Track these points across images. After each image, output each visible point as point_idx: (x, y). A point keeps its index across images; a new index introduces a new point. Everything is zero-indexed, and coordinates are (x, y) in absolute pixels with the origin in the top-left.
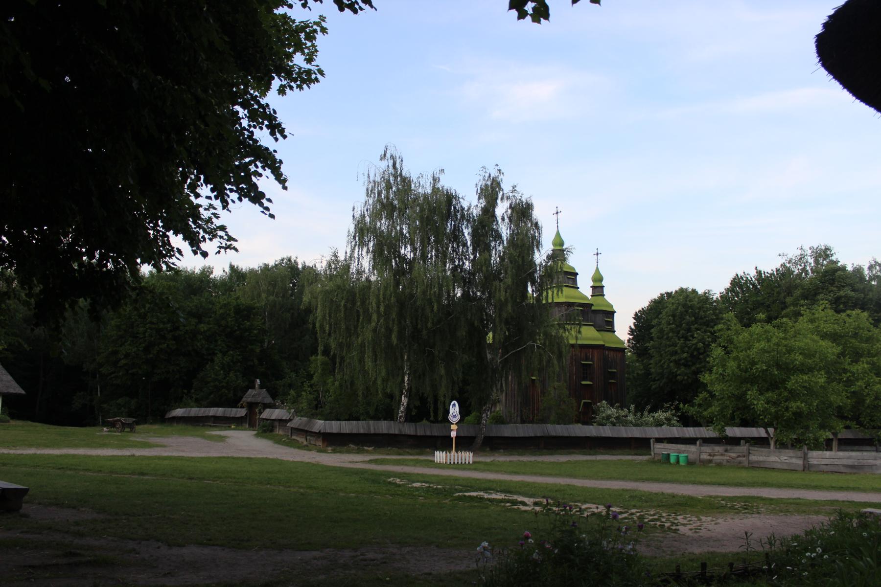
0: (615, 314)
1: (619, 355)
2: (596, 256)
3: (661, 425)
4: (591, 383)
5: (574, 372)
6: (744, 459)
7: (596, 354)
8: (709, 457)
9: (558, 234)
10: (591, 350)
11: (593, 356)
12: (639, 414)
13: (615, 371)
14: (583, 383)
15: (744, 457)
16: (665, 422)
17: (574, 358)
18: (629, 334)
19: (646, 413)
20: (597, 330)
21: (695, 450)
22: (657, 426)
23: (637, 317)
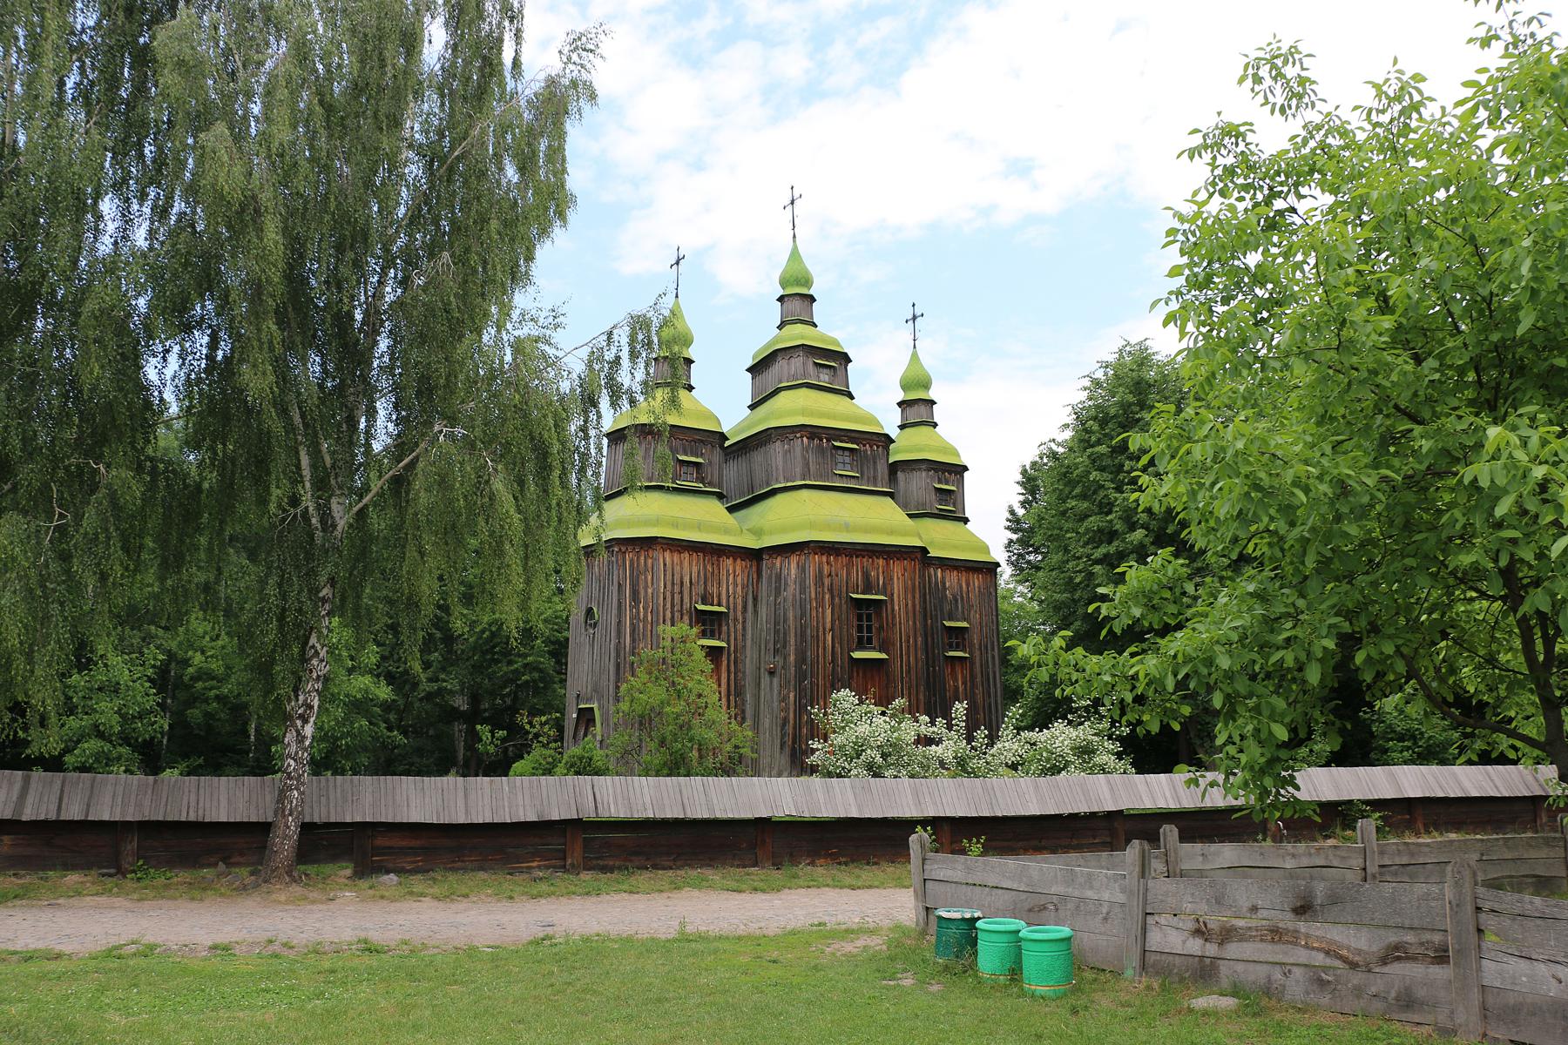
0: (966, 474)
1: (977, 581)
2: (911, 323)
3: (1055, 770)
4: (884, 656)
5: (828, 626)
6: (1439, 973)
7: (897, 569)
8: (1195, 946)
9: (795, 254)
10: (881, 562)
11: (889, 580)
12: (981, 734)
13: (965, 624)
14: (857, 655)
15: (1441, 958)
16: (1071, 758)
17: (827, 581)
18: (1008, 528)
19: (1007, 731)
20: (910, 516)
21: (1121, 898)
22: (1044, 772)
23: (1029, 482)
